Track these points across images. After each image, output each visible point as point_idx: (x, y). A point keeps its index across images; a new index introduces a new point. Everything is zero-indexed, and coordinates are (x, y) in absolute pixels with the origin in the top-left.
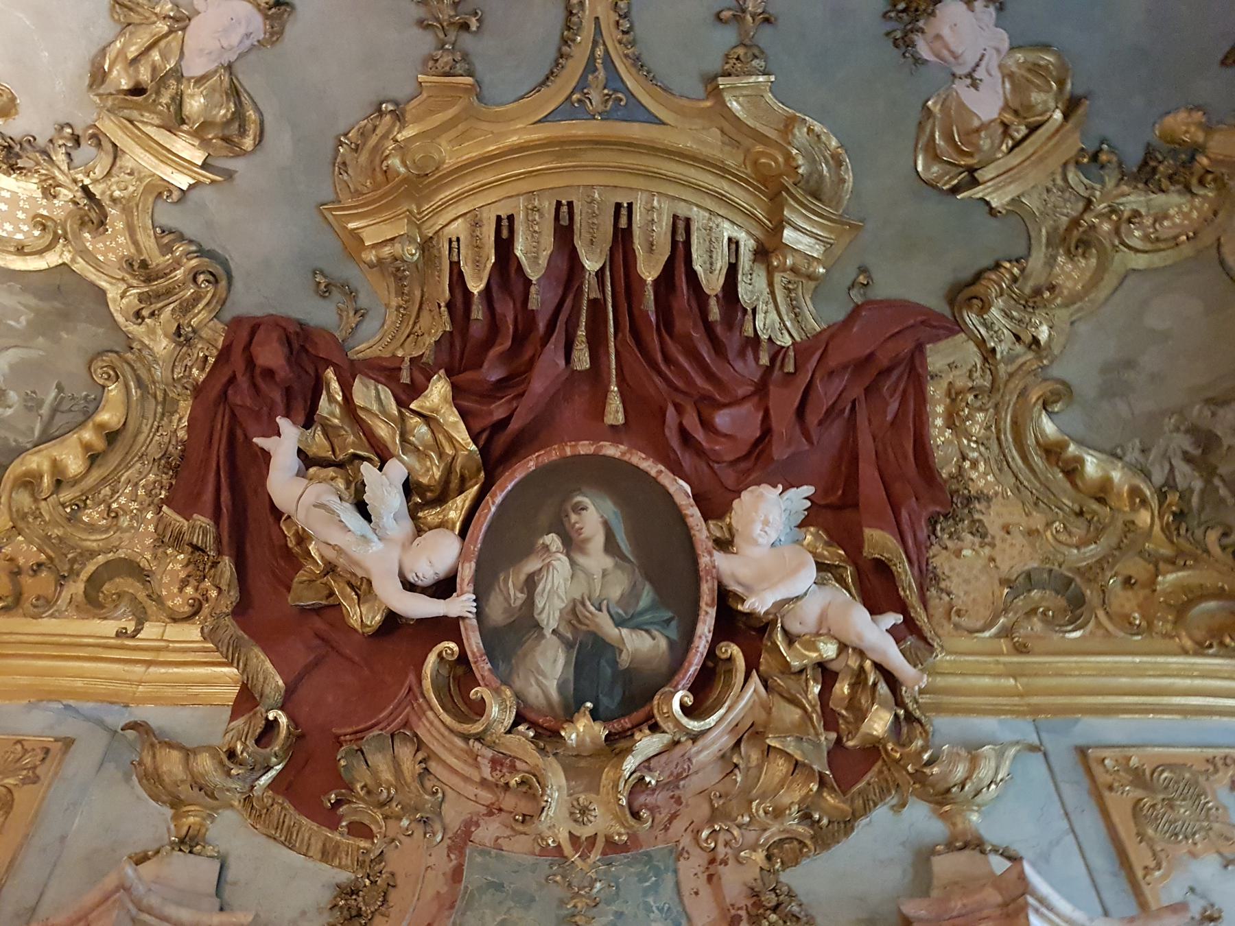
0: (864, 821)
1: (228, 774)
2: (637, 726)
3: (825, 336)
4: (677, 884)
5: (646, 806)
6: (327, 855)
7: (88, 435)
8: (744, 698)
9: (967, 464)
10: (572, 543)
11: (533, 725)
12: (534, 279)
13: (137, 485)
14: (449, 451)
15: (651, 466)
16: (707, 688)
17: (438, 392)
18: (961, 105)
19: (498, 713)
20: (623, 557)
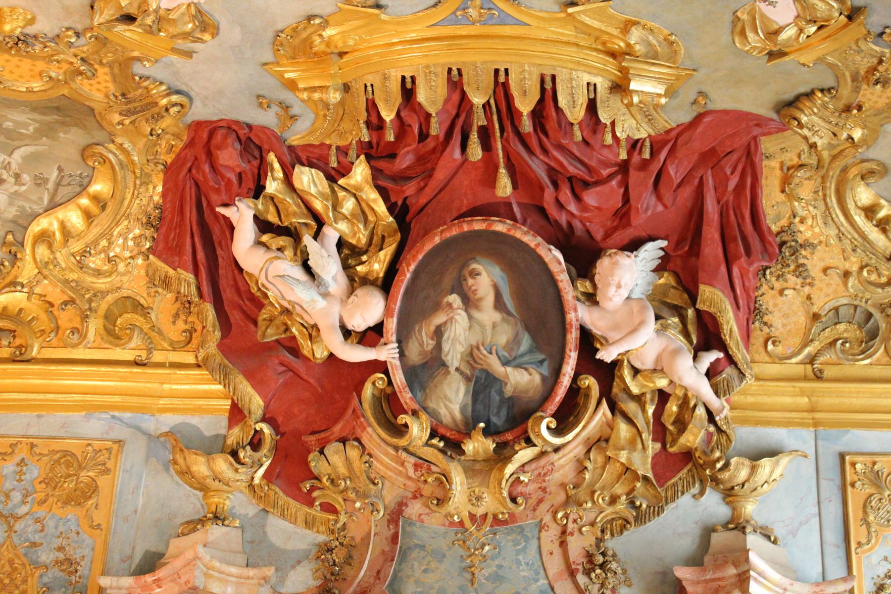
0: (672, 506)
1: (236, 470)
2: (516, 440)
3: (673, 134)
4: (540, 547)
5: (522, 494)
6: (309, 524)
7: (84, 201)
8: (596, 418)
9: (797, 220)
10: (469, 302)
11: (442, 438)
12: (432, 111)
13: (129, 239)
14: (371, 218)
15: (531, 240)
16: (567, 416)
17: (360, 172)
18: (763, 16)
19: (418, 430)
20: (509, 313)
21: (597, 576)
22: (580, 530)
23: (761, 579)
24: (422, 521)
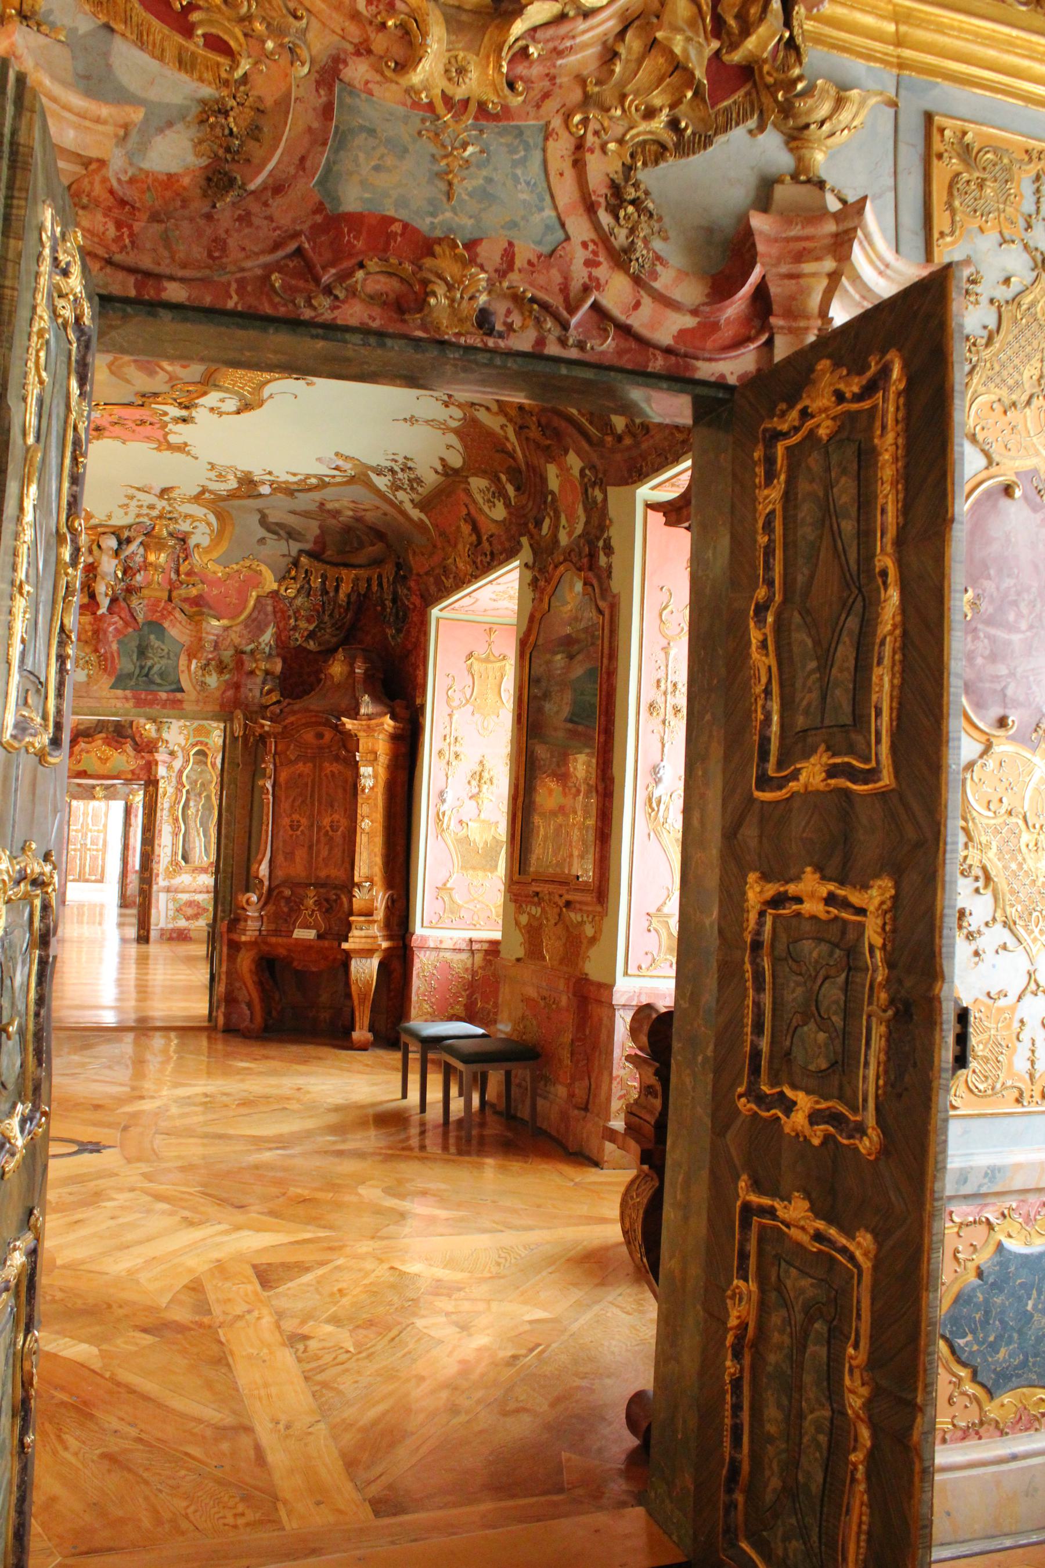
4: (545, 162)
5: (521, 78)
21: (627, 217)
22: (603, 148)
23: (865, 244)
24: (371, 93)
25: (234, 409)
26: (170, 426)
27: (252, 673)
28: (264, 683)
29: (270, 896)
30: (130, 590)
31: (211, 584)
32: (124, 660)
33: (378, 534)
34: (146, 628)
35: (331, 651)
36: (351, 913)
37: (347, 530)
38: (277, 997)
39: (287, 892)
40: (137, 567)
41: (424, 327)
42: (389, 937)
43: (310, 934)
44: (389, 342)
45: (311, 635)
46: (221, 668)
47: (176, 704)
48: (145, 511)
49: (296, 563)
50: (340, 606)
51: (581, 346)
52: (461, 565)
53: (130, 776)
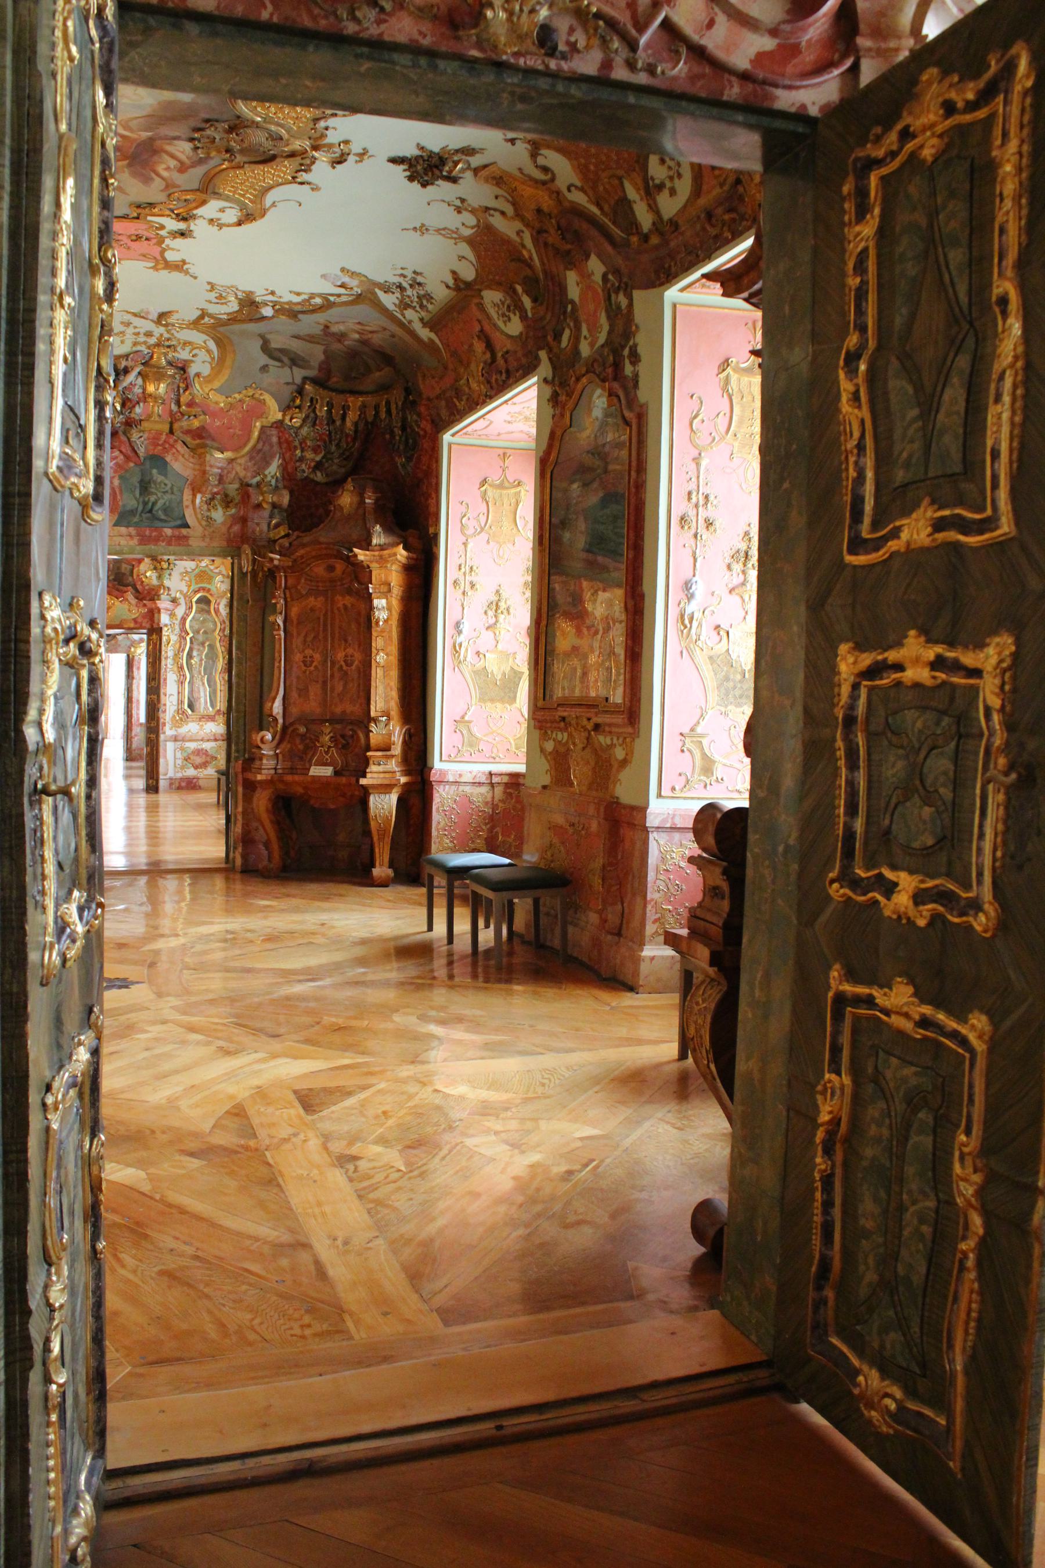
25: (235, 220)
26: (167, 241)
27: (259, 506)
28: (271, 517)
29: (285, 734)
30: (129, 423)
31: (214, 415)
32: (125, 495)
33: (385, 358)
34: (148, 463)
35: (337, 483)
36: (368, 748)
37: (353, 354)
38: (294, 835)
39: (302, 730)
40: (136, 399)
41: (479, 45)
42: (406, 773)
43: (327, 771)
44: (442, 64)
45: (319, 466)
46: (227, 502)
47: (182, 540)
48: (142, 339)
49: (300, 391)
50: (347, 435)
51: (651, 70)
52: (474, 385)
53: (132, 625)
